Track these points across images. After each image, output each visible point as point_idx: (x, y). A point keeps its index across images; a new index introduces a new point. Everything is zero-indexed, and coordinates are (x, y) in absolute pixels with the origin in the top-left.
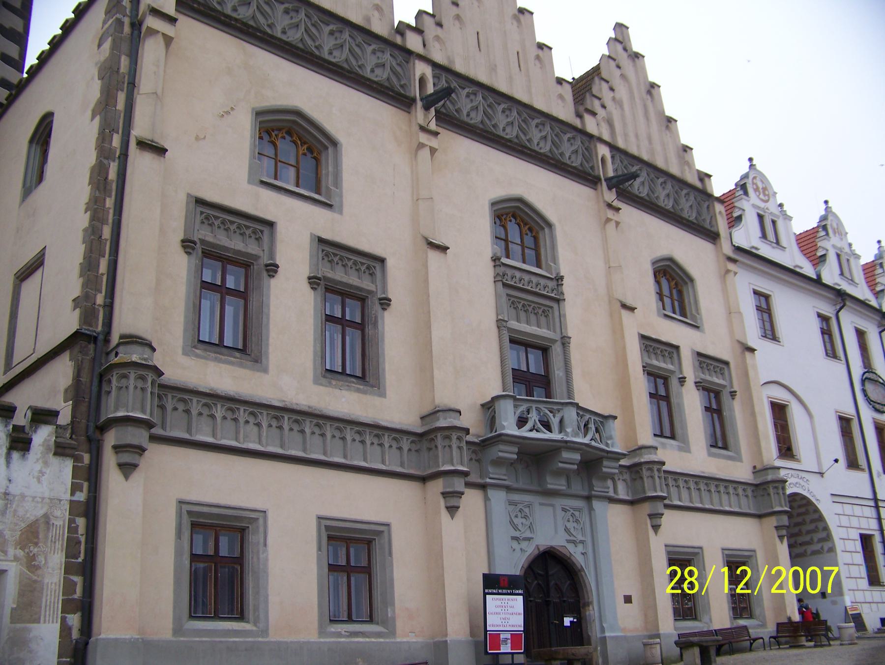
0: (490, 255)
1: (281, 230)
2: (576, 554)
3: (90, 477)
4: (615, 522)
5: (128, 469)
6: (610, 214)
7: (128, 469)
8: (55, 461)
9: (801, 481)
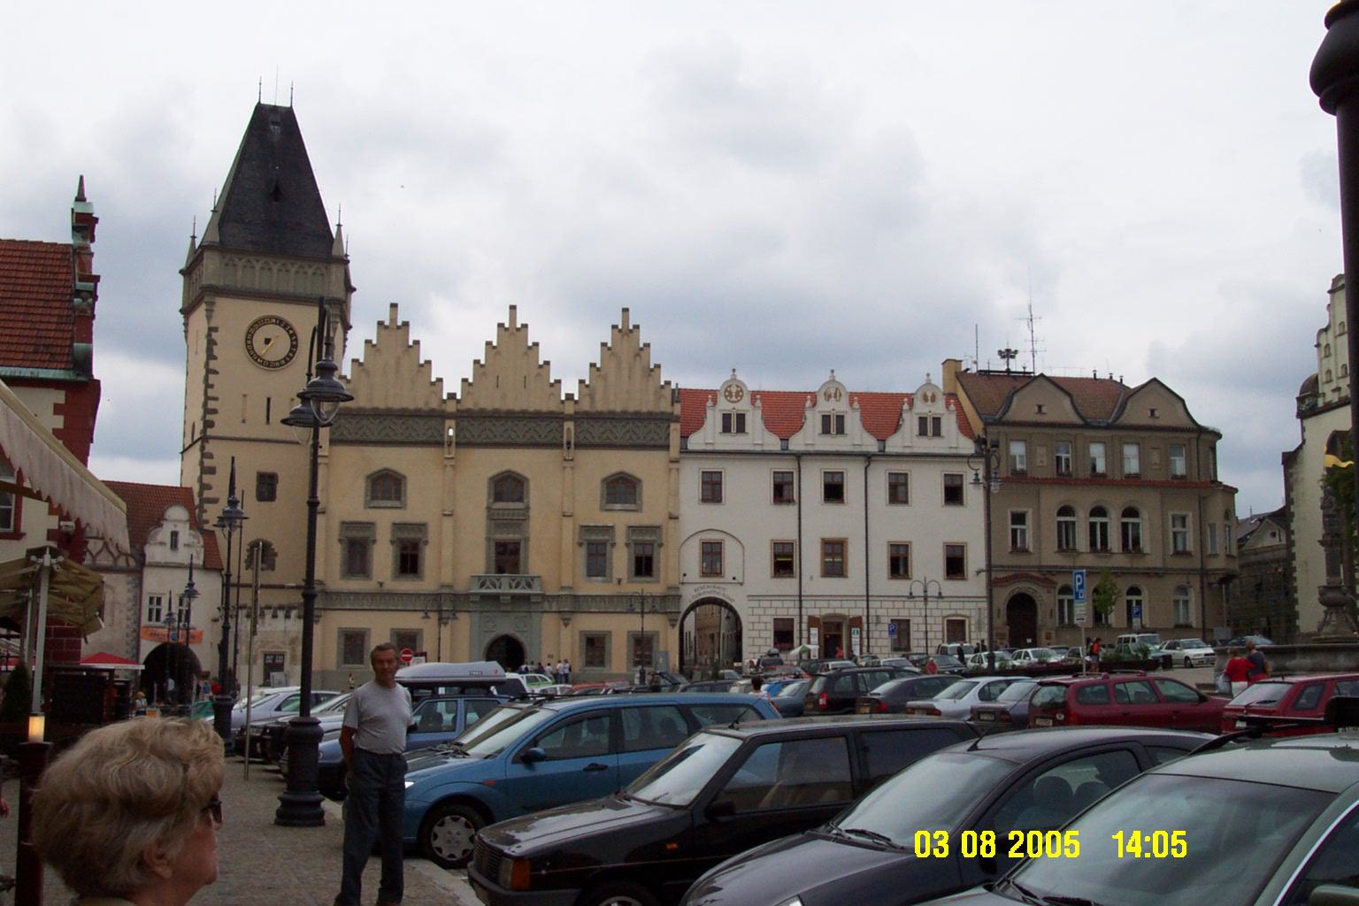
0: (485, 506)
1: (378, 525)
2: (521, 637)
4: (549, 623)
6: (566, 464)
8: (298, 620)
9: (718, 591)
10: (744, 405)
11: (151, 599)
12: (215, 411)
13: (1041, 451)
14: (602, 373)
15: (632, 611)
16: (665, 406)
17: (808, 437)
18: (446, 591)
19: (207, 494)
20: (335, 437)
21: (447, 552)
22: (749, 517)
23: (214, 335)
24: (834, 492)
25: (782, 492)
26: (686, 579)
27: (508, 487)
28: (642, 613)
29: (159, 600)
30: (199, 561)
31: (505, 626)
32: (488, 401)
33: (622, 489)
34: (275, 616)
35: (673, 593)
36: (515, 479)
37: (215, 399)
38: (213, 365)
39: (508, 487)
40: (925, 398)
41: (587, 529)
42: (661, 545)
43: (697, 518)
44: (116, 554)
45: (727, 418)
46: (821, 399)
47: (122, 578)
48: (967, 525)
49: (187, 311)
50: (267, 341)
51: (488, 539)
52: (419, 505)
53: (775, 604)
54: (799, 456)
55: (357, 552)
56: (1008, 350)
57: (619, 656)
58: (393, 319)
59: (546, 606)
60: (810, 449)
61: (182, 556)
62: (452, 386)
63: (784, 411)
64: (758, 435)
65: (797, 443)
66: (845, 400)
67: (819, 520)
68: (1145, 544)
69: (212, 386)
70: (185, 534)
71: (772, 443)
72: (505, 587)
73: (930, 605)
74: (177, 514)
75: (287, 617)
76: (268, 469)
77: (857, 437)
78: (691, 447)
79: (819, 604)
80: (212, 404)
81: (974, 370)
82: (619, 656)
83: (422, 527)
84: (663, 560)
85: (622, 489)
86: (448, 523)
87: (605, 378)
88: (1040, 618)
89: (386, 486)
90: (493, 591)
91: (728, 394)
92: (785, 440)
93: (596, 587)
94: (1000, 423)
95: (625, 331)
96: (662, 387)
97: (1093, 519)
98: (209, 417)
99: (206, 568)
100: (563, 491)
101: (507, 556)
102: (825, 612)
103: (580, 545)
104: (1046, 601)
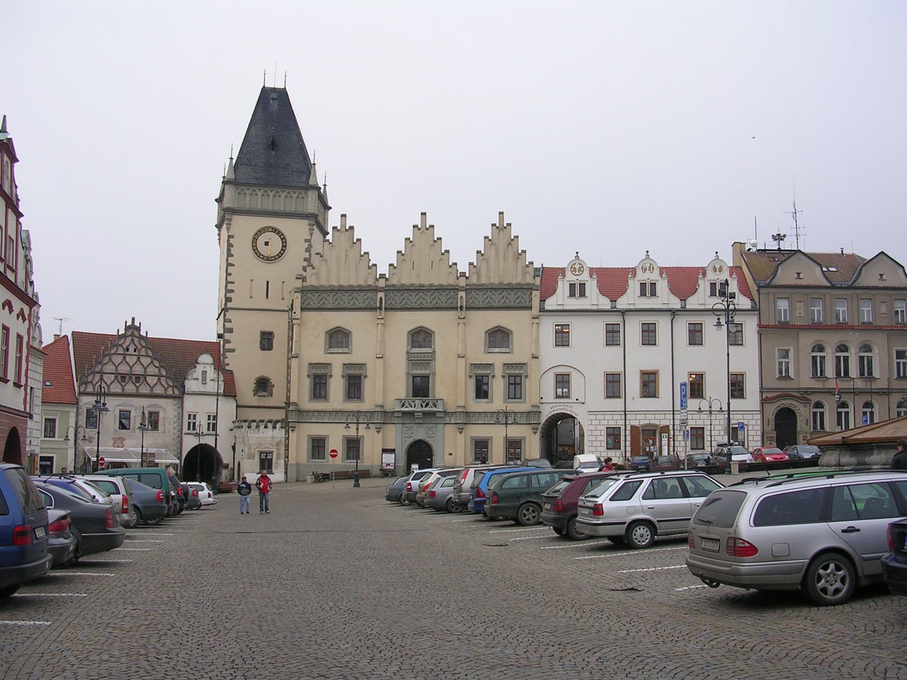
2: (430, 441)
3: (287, 432)
4: (450, 430)
5: (293, 431)
6: (460, 321)
7: (293, 431)
10: (584, 277)
11: (190, 415)
12: (232, 291)
13: (800, 306)
14: (485, 257)
15: (498, 423)
16: (529, 279)
17: (630, 298)
18: (379, 409)
19: (228, 346)
20: (304, 306)
21: (379, 383)
22: (589, 354)
23: (231, 240)
24: (649, 336)
25: (613, 336)
26: (543, 401)
27: (421, 337)
28: (506, 424)
29: (195, 416)
30: (221, 391)
31: (420, 433)
32: (406, 278)
33: (499, 337)
34: (266, 427)
35: (535, 410)
36: (425, 332)
37: (233, 283)
38: (231, 260)
39: (421, 337)
40: (715, 269)
41: (475, 366)
42: (526, 377)
43: (553, 357)
44: (166, 386)
45: (572, 286)
46: (639, 273)
47: (170, 400)
48: (747, 359)
49: (219, 226)
50: (267, 244)
51: (408, 374)
52: (362, 349)
53: (607, 417)
54: (623, 313)
55: (319, 384)
56: (779, 235)
57: (497, 453)
58: (343, 224)
59: (447, 420)
60: (632, 307)
61: (211, 387)
62: (383, 269)
63: (612, 281)
64: (594, 298)
65: (623, 303)
66: (656, 272)
67: (639, 358)
68: (876, 374)
69: (230, 274)
70: (211, 373)
71: (605, 303)
72: (417, 406)
73: (713, 417)
74: (206, 359)
75: (274, 427)
76: (267, 329)
77: (665, 298)
78: (547, 308)
79: (638, 417)
80: (230, 287)
81: (754, 249)
82: (497, 453)
83: (362, 366)
84: (529, 386)
85: (499, 337)
86: (380, 361)
87: (487, 261)
88: (798, 425)
89: (338, 338)
90: (410, 409)
91: (573, 270)
92: (613, 301)
93: (481, 406)
94: (769, 286)
95: (501, 228)
96: (527, 266)
97: (838, 354)
98: (228, 295)
99: (225, 395)
100: (458, 341)
101: (420, 387)
102: (643, 422)
103: (471, 377)
104: (804, 413)
